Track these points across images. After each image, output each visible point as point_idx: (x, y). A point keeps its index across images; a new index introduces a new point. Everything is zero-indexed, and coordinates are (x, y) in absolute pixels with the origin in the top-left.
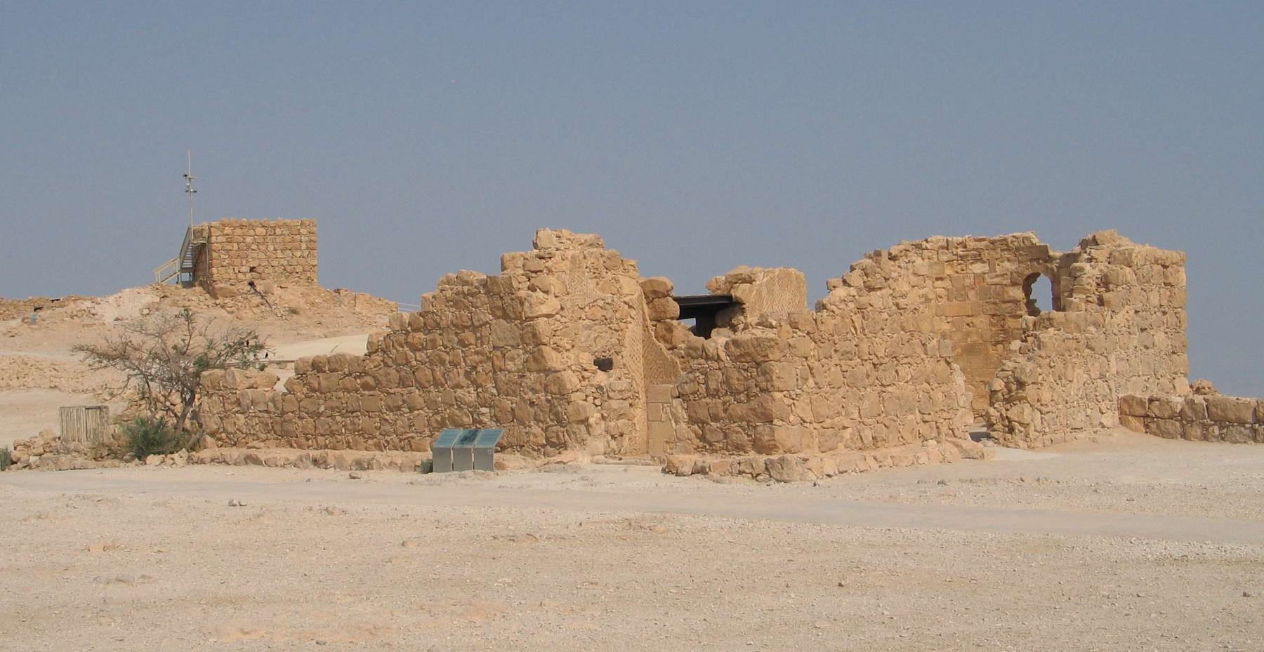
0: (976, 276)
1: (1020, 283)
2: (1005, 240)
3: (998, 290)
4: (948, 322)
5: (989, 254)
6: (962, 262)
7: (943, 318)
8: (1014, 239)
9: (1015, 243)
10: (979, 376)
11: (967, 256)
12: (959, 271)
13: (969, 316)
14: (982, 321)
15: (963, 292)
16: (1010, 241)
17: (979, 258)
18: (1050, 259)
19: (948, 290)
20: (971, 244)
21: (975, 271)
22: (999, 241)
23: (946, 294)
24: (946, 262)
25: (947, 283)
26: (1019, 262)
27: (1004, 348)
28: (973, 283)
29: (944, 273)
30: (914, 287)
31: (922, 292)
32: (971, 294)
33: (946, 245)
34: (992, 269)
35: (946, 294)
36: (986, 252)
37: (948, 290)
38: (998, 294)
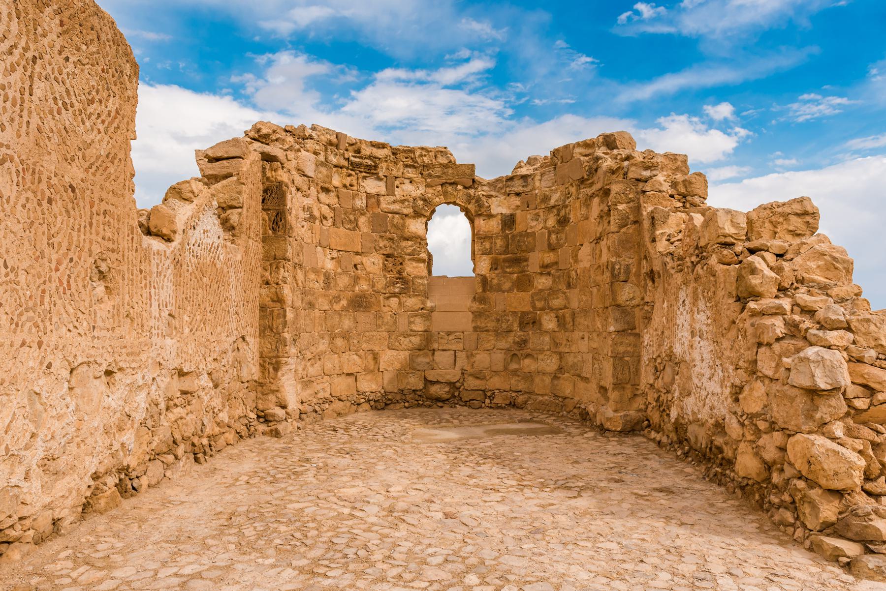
0: (369, 196)
1: (426, 214)
2: (412, 151)
3: (396, 221)
4: (333, 259)
5: (387, 169)
6: (353, 173)
7: (328, 251)
8: (424, 153)
9: (426, 159)
10: (367, 342)
11: (359, 165)
12: (348, 185)
13: (357, 253)
14: (373, 263)
15: (352, 217)
16: (418, 153)
17: (375, 172)
18: (475, 183)
19: (334, 210)
20: (367, 151)
21: (369, 190)
22: (405, 151)
23: (333, 215)
24: (335, 166)
25: (331, 199)
26: (428, 186)
27: (400, 303)
28: (364, 206)
29: (330, 183)
30: (298, 189)
31: (307, 202)
32: (362, 220)
33: (335, 140)
34: (390, 192)
35: (333, 215)
36: (384, 165)
37: (334, 210)
38: (396, 227)
